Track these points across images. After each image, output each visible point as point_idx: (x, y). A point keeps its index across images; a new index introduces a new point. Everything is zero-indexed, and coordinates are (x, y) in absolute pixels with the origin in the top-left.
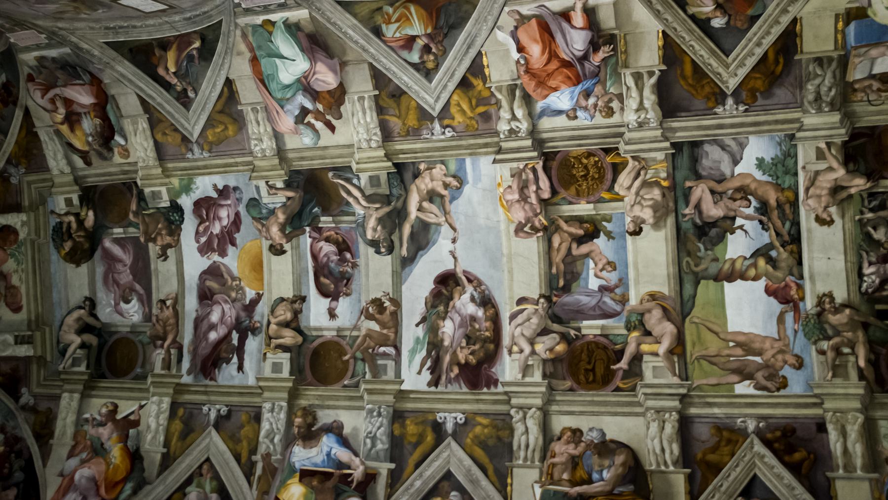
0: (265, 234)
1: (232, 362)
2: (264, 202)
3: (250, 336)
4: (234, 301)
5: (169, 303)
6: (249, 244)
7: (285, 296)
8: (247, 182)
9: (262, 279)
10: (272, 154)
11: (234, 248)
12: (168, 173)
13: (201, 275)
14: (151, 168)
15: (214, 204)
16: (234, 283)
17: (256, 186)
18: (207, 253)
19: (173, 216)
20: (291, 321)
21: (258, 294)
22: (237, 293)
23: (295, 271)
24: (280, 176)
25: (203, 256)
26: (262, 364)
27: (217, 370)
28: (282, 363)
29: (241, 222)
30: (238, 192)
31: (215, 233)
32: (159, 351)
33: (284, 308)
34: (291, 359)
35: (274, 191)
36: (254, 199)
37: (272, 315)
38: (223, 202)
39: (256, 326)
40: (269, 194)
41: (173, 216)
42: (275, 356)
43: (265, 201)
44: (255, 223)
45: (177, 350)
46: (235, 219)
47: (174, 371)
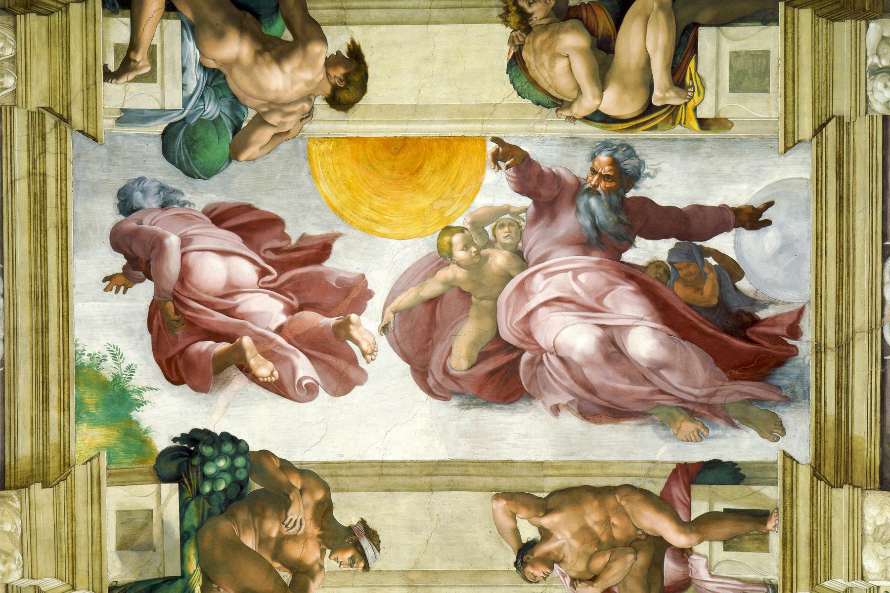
0: (291, 122)
1: (732, 255)
2: (178, 104)
3: (643, 190)
4: (521, 257)
5: (529, 533)
6: (325, 188)
7: (505, 52)
8: (103, 151)
9: (448, 143)
10: (9, 34)
11: (337, 246)
12: (54, 464)
13: (430, 392)
14: (30, 530)
15: (176, 299)
16: (460, 254)
17: (119, 121)
18: (354, 361)
19: (213, 479)
20: (592, 32)
21: (497, 158)
22: (490, 244)
23: (420, 14)
24: (88, 20)
25: (362, 377)
26: (736, 131)
27: (762, 314)
28: (735, 55)
29: (249, 208)
30: (138, 196)
31: (283, 319)
32: (699, 567)
33: (545, 58)
34: (719, 22)
35: (140, 57)
36: (167, 136)
37: (570, 105)
38: (172, 265)
39: (606, 170)
40: (150, 77)
41: (213, 479)
42: (710, 84)
43: (174, 99)
44: (252, 151)
45: (695, 488)
46: (232, 229)
47: (771, 494)
